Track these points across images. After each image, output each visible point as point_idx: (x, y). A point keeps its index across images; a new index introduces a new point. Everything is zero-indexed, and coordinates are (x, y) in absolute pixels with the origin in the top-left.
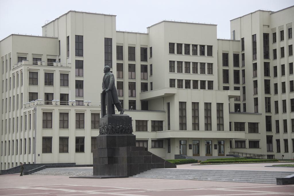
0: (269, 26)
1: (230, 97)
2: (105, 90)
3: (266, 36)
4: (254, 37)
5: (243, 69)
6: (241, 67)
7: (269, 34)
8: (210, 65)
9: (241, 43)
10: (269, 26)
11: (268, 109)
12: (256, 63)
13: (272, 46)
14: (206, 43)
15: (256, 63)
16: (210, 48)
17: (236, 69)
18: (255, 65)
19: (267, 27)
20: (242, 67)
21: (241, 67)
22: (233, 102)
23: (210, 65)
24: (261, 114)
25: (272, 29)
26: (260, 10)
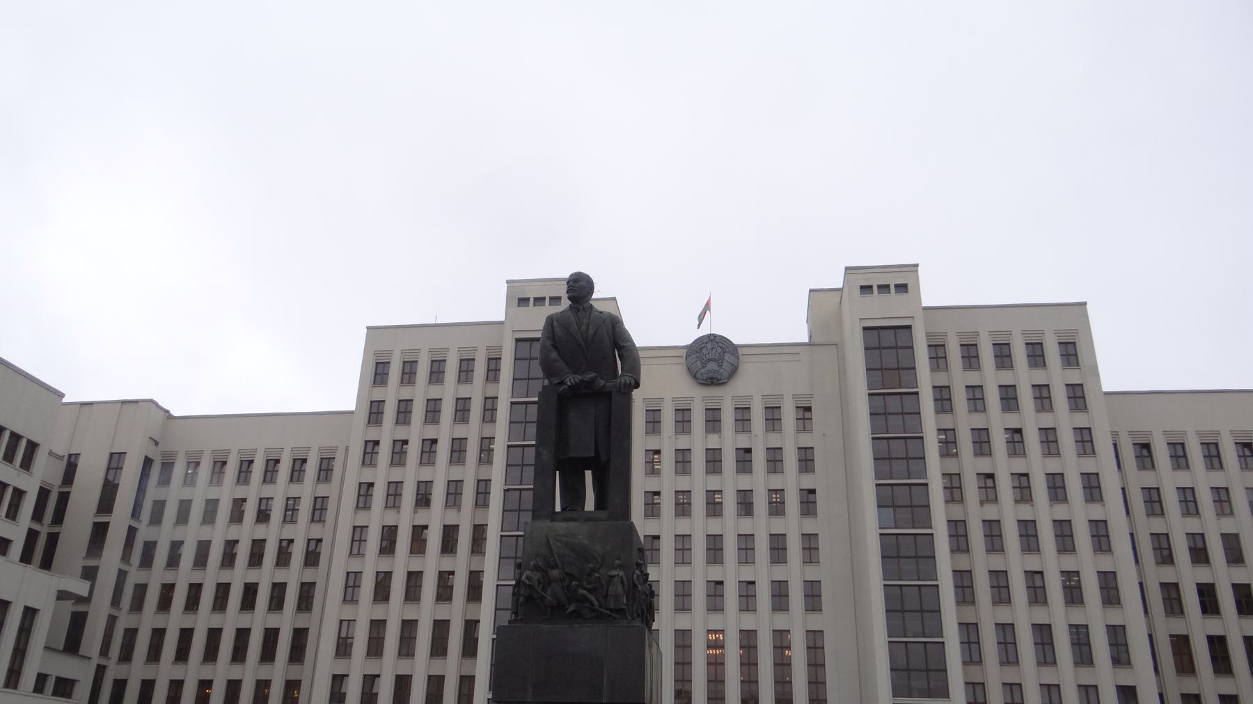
0: (156, 443)
1: (62, 595)
2: (592, 381)
3: (148, 462)
4: (115, 461)
5: (55, 530)
6: (46, 525)
7: (153, 461)
8: (19, 494)
9: (63, 465)
10: (156, 443)
11: (105, 651)
12: (108, 523)
13: (153, 492)
14: (29, 433)
15: (108, 523)
16: (32, 447)
17: (36, 527)
18: (100, 531)
19: (154, 443)
20: (50, 526)
21: (46, 525)
22: (69, 607)
23: (19, 494)
24: (90, 658)
25: (164, 454)
26: (151, 401)
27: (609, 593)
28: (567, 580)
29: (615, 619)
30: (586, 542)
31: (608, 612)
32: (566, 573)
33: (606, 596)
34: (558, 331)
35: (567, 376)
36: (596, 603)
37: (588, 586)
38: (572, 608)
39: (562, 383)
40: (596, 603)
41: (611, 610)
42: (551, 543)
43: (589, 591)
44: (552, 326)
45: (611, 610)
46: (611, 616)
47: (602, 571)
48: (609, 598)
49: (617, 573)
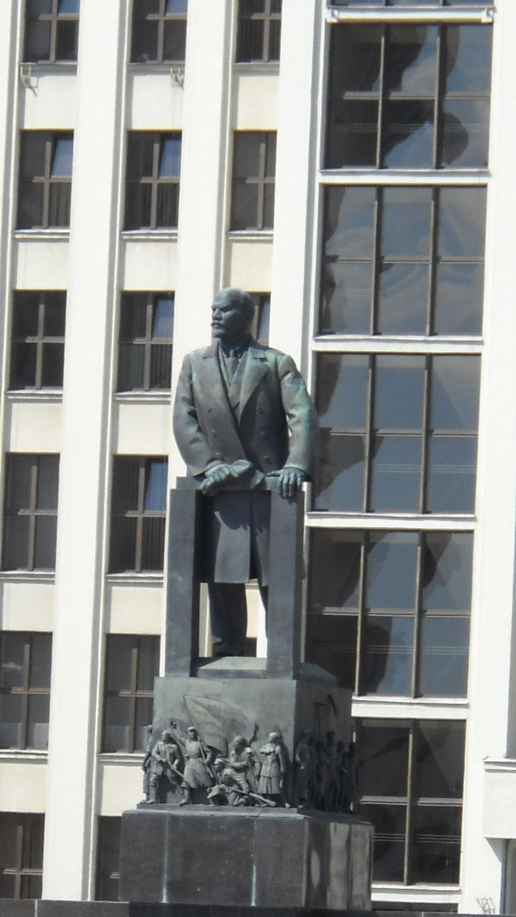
27: (262, 774)
28: (209, 756)
29: (269, 806)
30: (237, 707)
31: (261, 798)
32: (210, 747)
33: (259, 777)
34: (200, 396)
35: (210, 465)
36: (245, 786)
37: (237, 765)
38: (215, 791)
39: (202, 477)
40: (245, 786)
41: (264, 796)
42: (190, 707)
43: (238, 770)
44: (190, 377)
45: (264, 796)
46: (265, 803)
47: (254, 744)
48: (262, 778)
49: (272, 750)
